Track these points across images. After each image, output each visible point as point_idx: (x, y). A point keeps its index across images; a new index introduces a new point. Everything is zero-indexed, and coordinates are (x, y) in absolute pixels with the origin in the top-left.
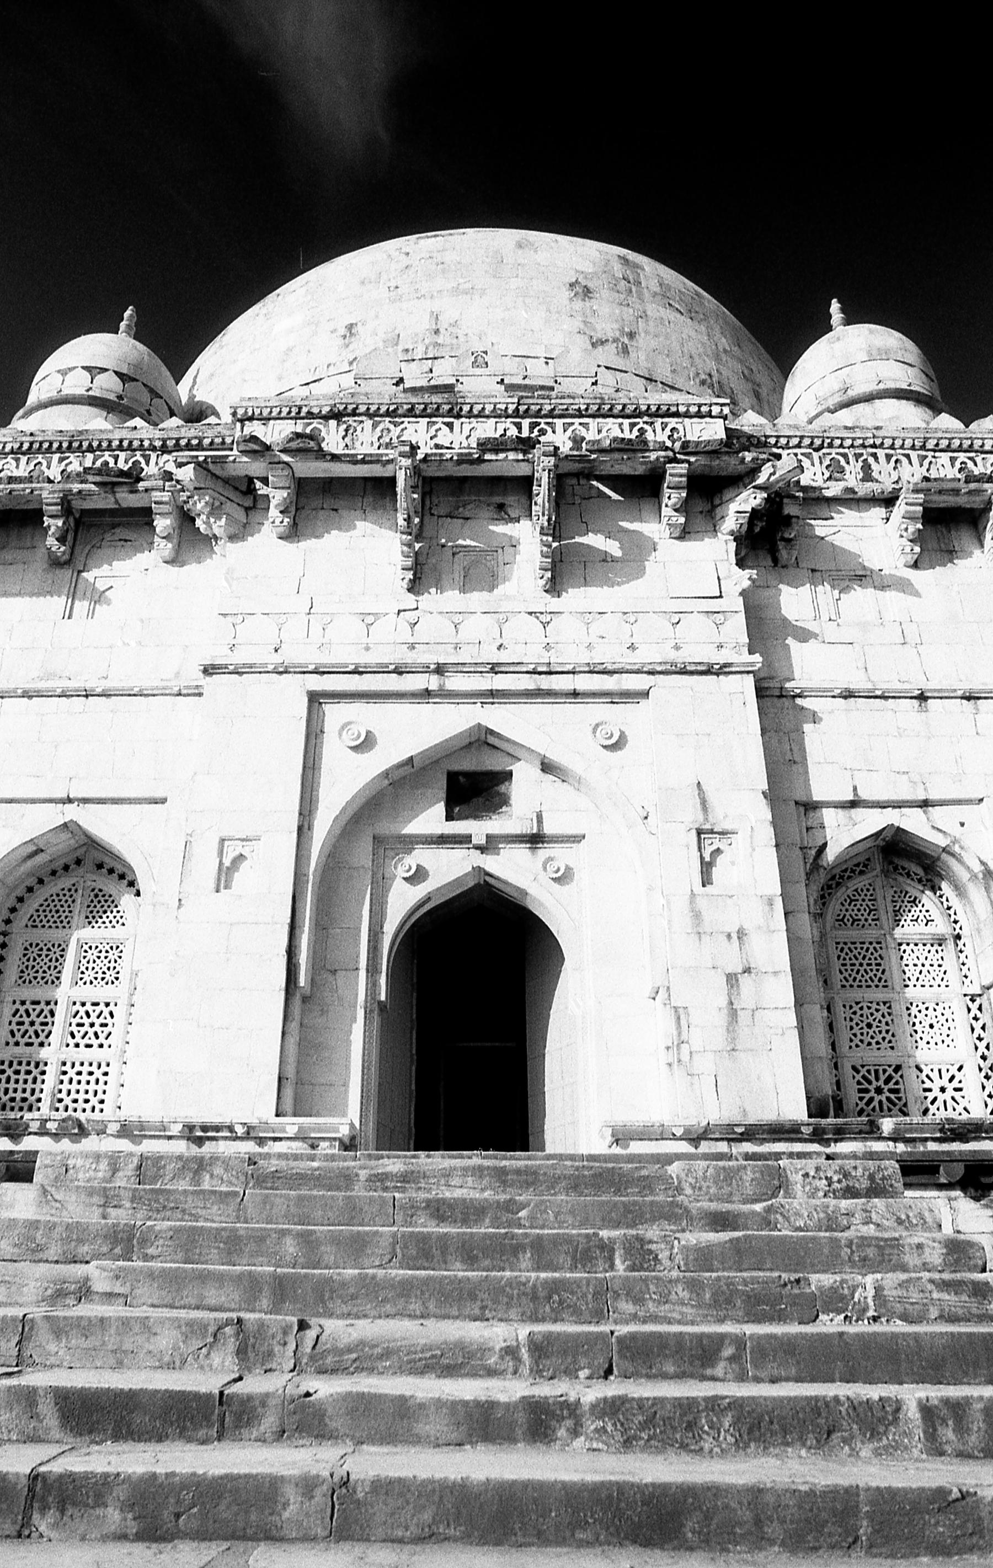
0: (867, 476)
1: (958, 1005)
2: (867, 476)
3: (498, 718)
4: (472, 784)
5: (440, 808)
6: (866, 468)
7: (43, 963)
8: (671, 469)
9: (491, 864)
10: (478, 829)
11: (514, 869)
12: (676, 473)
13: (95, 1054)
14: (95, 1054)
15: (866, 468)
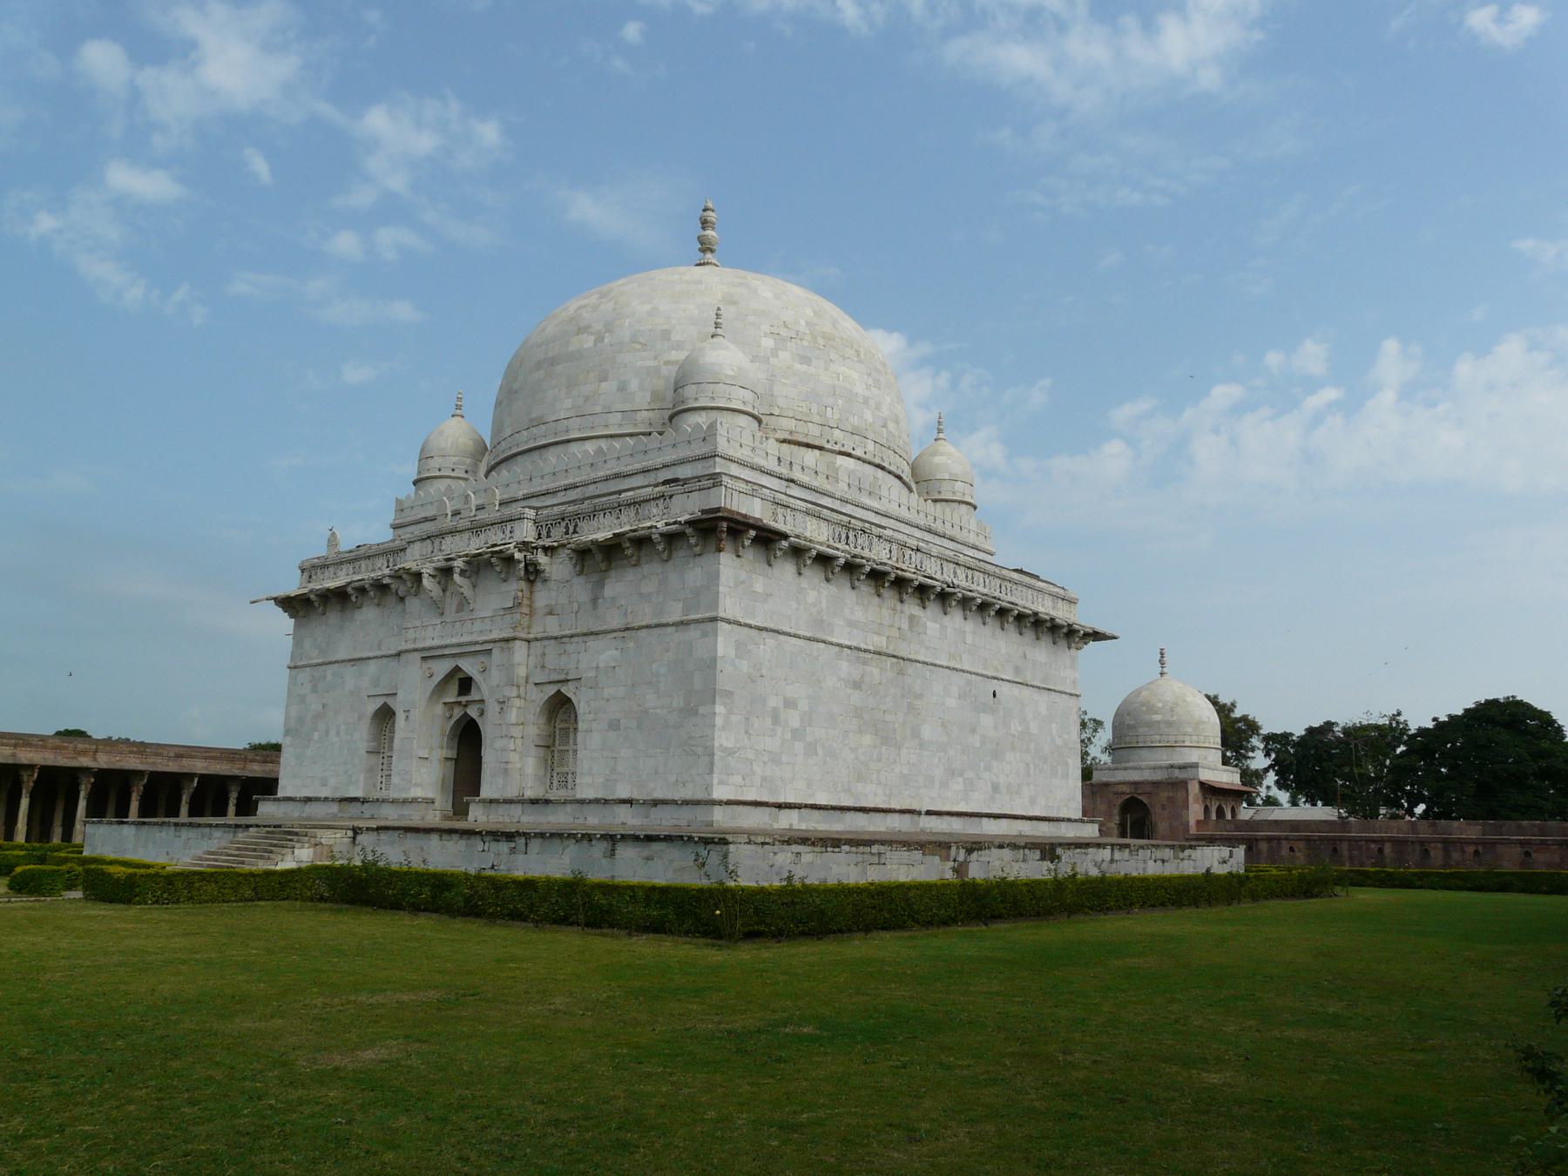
0: (575, 532)
10: (463, 699)
11: (473, 712)
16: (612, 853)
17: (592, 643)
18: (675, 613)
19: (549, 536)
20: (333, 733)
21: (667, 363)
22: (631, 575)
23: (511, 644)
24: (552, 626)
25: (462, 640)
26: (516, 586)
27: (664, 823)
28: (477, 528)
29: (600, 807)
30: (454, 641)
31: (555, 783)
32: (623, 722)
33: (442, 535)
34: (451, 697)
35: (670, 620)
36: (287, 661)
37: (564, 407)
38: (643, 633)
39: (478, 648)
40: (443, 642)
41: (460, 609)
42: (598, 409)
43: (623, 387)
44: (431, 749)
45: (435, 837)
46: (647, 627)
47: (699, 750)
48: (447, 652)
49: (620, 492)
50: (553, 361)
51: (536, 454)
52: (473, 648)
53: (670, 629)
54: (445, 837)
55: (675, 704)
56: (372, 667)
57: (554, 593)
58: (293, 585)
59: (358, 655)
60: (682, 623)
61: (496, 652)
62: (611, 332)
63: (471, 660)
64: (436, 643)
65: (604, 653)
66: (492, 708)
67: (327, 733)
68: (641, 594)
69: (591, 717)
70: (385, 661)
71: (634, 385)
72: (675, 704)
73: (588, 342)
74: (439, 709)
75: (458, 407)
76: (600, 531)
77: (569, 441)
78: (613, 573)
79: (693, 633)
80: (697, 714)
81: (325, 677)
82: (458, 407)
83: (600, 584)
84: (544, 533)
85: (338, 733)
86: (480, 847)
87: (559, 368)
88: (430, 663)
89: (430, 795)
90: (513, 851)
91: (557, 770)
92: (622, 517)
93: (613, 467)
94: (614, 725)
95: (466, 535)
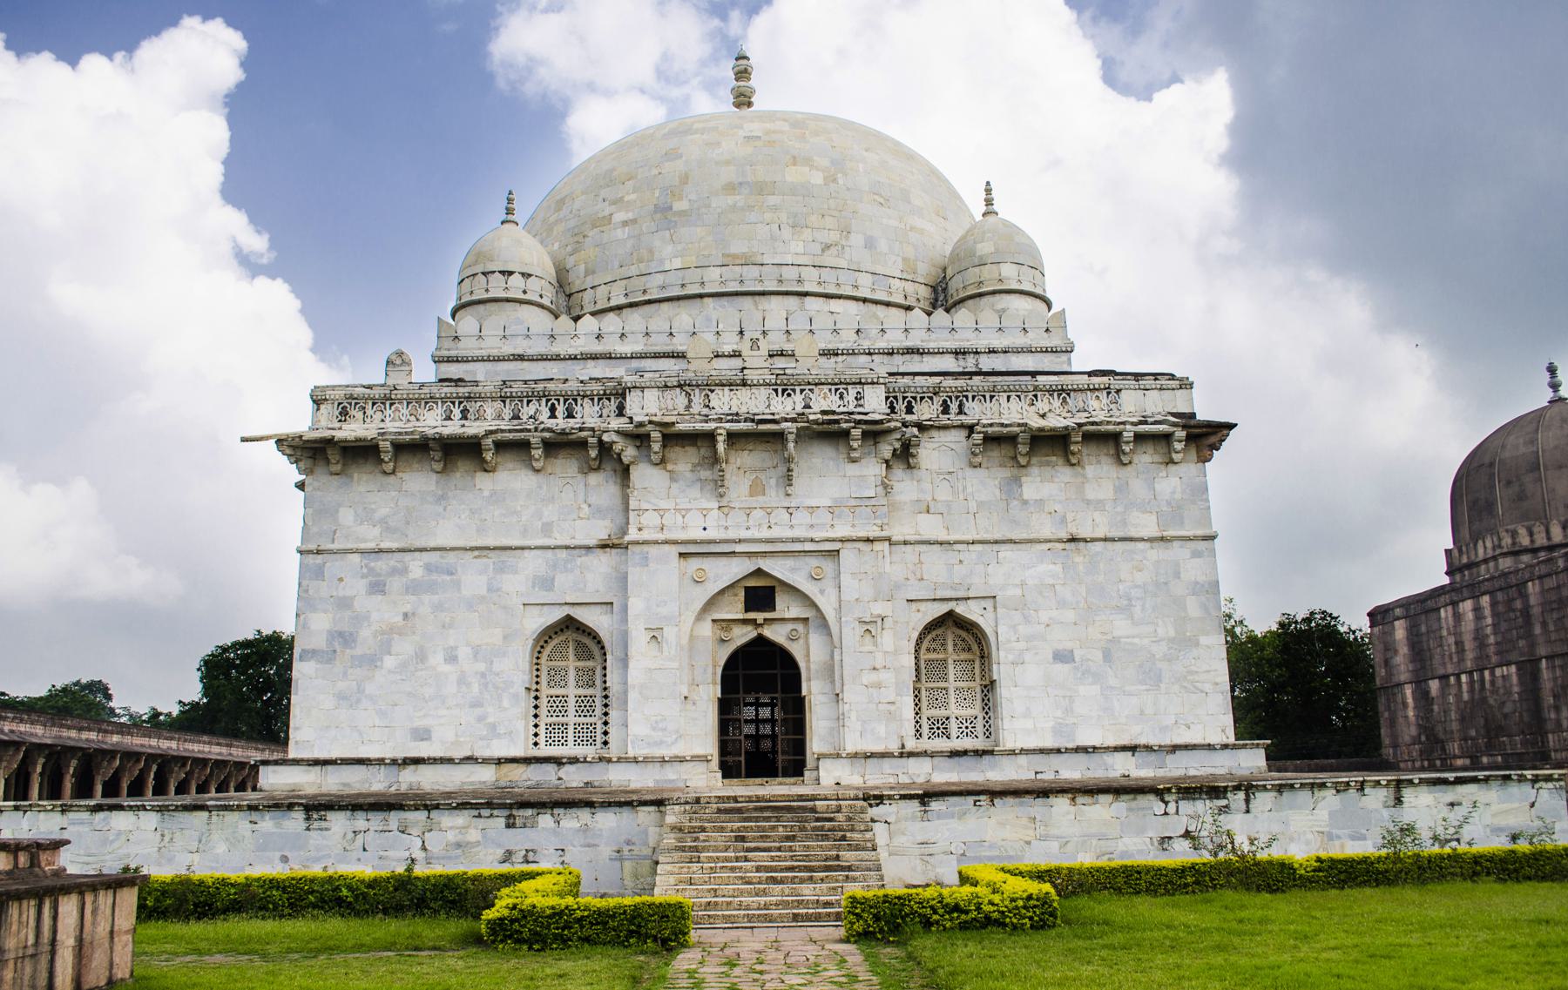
0: (961, 412)
1: (978, 690)
2: (961, 412)
3: (767, 565)
4: (760, 595)
5: (741, 606)
6: (961, 406)
7: (557, 678)
8: (854, 432)
9: (769, 632)
10: (760, 616)
11: (776, 634)
12: (856, 433)
13: (588, 720)
14: (588, 720)
15: (961, 406)
16: (1399, 801)
17: (1006, 552)
18: (1147, 525)
19: (909, 410)
20: (436, 659)
21: (912, 229)
22: (1064, 474)
23: (878, 546)
24: (930, 527)
25: (775, 533)
26: (871, 469)
27: (1192, 772)
28: (784, 387)
29: (1082, 757)
30: (757, 535)
31: (925, 730)
32: (1078, 654)
33: (709, 386)
34: (734, 609)
35: (1145, 534)
36: (297, 542)
37: (795, 248)
38: (1099, 546)
39: (809, 546)
40: (731, 535)
41: (757, 489)
42: (843, 264)
43: (870, 244)
44: (694, 684)
45: (1061, 803)
46: (1105, 540)
47: (1208, 687)
48: (739, 548)
49: (1034, 374)
50: (761, 189)
51: (747, 302)
52: (798, 547)
53: (1140, 545)
54: (1080, 799)
55: (1161, 632)
56: (532, 564)
57: (927, 486)
58: (301, 421)
59: (491, 542)
60: (1162, 539)
61: (848, 554)
62: (845, 174)
63: (790, 562)
64: (712, 534)
65: (1036, 568)
66: (850, 635)
67: (421, 656)
68: (1088, 502)
69: (1022, 645)
70: (563, 554)
71: (883, 245)
72: (1161, 632)
73: (817, 179)
74: (707, 629)
75: (509, 211)
76: (1014, 413)
77: (806, 294)
78: (1035, 470)
79: (1179, 552)
80: (1197, 644)
81: (405, 571)
82: (509, 211)
83: (1017, 480)
84: (901, 406)
85: (452, 658)
86: (1159, 807)
87: (773, 200)
88: (694, 564)
89: (700, 751)
90: (1225, 810)
91: (926, 713)
92: (1039, 404)
93: (895, 339)
94: (1063, 657)
95: (764, 392)
